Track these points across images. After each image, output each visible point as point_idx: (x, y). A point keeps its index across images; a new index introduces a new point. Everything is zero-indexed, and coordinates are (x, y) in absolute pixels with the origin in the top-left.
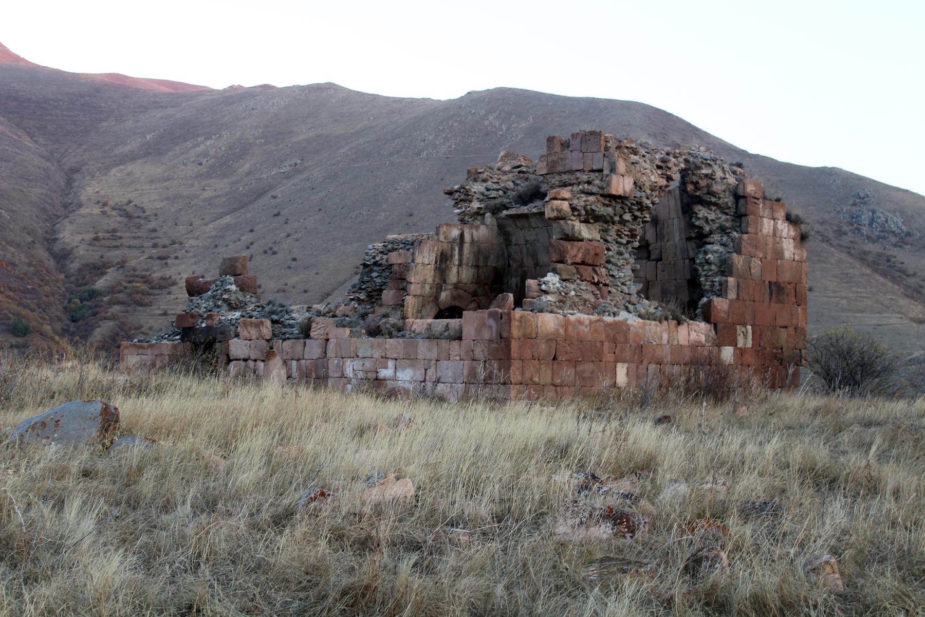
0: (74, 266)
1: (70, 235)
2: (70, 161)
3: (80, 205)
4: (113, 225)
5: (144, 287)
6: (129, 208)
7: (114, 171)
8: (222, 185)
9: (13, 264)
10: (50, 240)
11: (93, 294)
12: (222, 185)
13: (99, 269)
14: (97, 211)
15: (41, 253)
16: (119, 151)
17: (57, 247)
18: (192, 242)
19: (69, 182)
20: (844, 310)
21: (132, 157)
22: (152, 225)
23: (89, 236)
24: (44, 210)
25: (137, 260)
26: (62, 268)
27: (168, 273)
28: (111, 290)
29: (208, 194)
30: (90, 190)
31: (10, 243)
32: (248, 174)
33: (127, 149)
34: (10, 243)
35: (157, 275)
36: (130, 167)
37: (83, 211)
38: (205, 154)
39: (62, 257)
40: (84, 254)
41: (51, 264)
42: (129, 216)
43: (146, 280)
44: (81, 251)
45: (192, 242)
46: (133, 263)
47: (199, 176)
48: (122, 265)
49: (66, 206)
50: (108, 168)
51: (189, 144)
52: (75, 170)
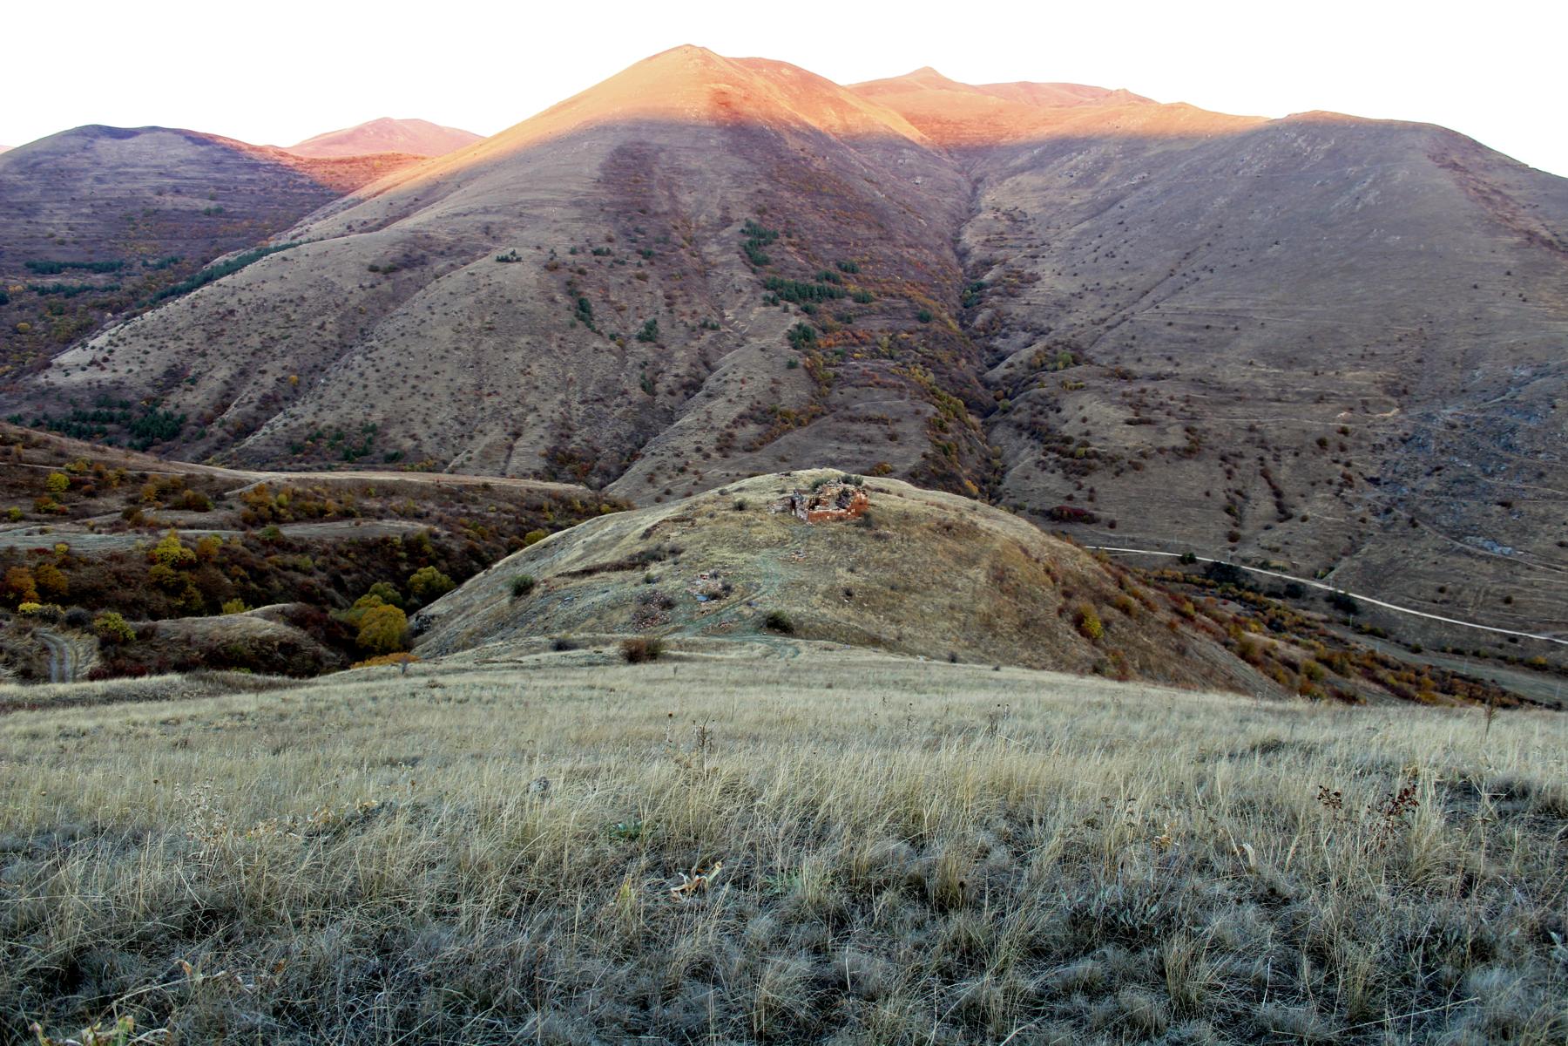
0: (971, 262)
1: (969, 238)
2: (976, 173)
3: (980, 211)
4: (1002, 228)
5: (1016, 281)
6: (1015, 214)
7: (1007, 182)
8: (1086, 194)
9: (925, 263)
10: (955, 241)
11: (981, 287)
12: (1086, 194)
13: (988, 265)
14: (991, 216)
15: (948, 252)
16: (1013, 163)
17: (959, 248)
18: (1057, 244)
19: (975, 189)
20: (1548, 318)
21: (1021, 170)
22: (1031, 228)
23: (983, 238)
24: (953, 216)
25: (1016, 258)
26: (962, 264)
27: (1037, 269)
28: (993, 284)
29: (1074, 202)
30: (988, 198)
31: (926, 246)
32: (1107, 185)
33: (1018, 162)
34: (926, 246)
35: (1027, 271)
36: (1019, 178)
37: (981, 216)
38: (1075, 168)
39: (963, 255)
40: (978, 253)
41: (955, 260)
42: (1014, 220)
43: (1020, 275)
44: (976, 251)
45: (1057, 244)
46: (1012, 261)
47: (1070, 186)
48: (1004, 262)
49: (970, 211)
50: (1003, 179)
51: (1065, 158)
52: (979, 180)
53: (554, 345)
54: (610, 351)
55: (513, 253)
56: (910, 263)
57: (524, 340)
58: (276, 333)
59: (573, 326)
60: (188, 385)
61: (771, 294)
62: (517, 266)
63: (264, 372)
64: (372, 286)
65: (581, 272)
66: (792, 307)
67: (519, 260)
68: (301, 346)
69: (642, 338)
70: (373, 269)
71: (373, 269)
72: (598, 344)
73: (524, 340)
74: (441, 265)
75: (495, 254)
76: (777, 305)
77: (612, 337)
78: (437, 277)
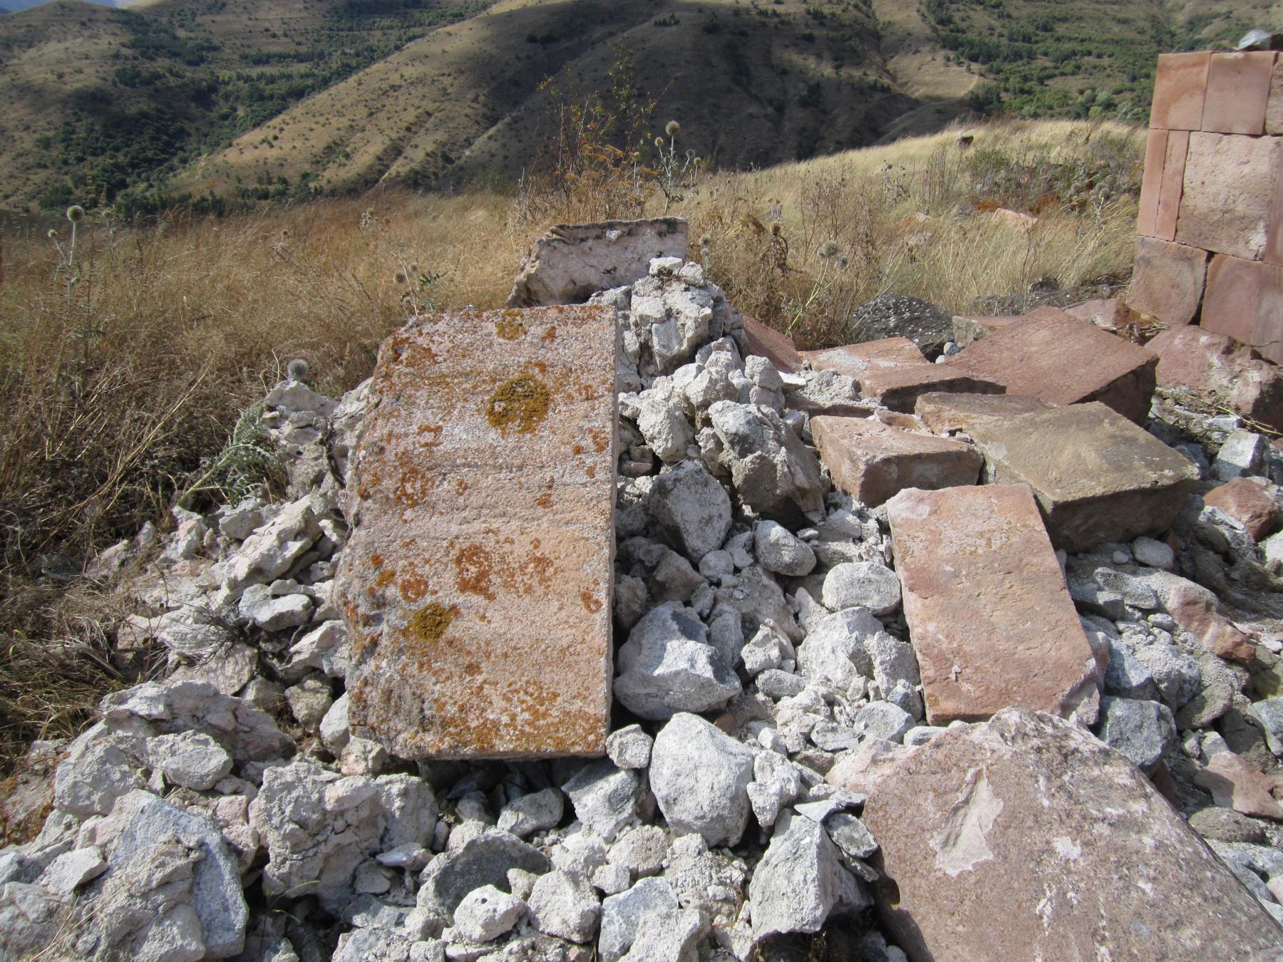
48: (1228, 16)
53: (705, 112)
54: (766, 116)
55: (673, 17)
56: (1114, 19)
57: (673, 106)
58: (430, 107)
59: (729, 91)
60: (343, 160)
61: (952, 55)
62: (674, 28)
63: (416, 146)
64: (528, 57)
65: (743, 34)
66: (975, 66)
67: (677, 23)
68: (453, 119)
69: (804, 103)
70: (532, 39)
71: (532, 39)
72: (753, 109)
73: (673, 106)
74: (599, 32)
75: (653, 20)
76: (960, 64)
77: (771, 102)
78: (594, 44)
